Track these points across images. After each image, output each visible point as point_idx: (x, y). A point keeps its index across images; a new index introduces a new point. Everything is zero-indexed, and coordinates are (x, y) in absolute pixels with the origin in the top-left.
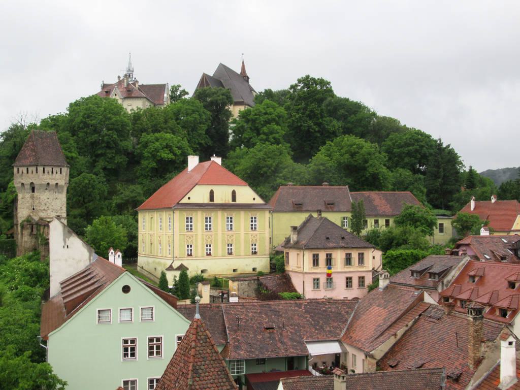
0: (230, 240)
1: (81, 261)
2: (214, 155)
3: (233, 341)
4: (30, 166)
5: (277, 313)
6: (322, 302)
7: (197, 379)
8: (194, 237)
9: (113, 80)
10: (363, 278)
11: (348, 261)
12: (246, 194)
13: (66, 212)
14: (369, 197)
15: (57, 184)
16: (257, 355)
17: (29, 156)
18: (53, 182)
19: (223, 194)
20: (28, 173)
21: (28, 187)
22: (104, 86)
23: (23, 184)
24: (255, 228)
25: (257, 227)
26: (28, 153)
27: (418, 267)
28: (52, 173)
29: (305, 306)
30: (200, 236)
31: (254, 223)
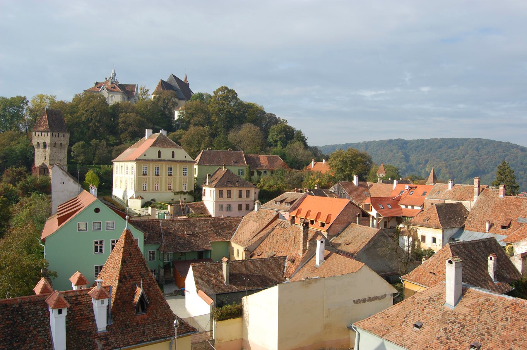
0: (170, 182)
1: (72, 192)
3: (166, 241)
6: (221, 219)
7: (125, 266)
8: (148, 179)
9: (102, 80)
10: (249, 205)
11: (240, 196)
12: (181, 154)
13: (67, 161)
15: (61, 143)
19: (166, 153)
20: (42, 136)
21: (41, 145)
22: (97, 84)
23: (38, 143)
24: (186, 175)
27: (279, 198)
28: (58, 136)
29: (211, 221)
30: (151, 179)
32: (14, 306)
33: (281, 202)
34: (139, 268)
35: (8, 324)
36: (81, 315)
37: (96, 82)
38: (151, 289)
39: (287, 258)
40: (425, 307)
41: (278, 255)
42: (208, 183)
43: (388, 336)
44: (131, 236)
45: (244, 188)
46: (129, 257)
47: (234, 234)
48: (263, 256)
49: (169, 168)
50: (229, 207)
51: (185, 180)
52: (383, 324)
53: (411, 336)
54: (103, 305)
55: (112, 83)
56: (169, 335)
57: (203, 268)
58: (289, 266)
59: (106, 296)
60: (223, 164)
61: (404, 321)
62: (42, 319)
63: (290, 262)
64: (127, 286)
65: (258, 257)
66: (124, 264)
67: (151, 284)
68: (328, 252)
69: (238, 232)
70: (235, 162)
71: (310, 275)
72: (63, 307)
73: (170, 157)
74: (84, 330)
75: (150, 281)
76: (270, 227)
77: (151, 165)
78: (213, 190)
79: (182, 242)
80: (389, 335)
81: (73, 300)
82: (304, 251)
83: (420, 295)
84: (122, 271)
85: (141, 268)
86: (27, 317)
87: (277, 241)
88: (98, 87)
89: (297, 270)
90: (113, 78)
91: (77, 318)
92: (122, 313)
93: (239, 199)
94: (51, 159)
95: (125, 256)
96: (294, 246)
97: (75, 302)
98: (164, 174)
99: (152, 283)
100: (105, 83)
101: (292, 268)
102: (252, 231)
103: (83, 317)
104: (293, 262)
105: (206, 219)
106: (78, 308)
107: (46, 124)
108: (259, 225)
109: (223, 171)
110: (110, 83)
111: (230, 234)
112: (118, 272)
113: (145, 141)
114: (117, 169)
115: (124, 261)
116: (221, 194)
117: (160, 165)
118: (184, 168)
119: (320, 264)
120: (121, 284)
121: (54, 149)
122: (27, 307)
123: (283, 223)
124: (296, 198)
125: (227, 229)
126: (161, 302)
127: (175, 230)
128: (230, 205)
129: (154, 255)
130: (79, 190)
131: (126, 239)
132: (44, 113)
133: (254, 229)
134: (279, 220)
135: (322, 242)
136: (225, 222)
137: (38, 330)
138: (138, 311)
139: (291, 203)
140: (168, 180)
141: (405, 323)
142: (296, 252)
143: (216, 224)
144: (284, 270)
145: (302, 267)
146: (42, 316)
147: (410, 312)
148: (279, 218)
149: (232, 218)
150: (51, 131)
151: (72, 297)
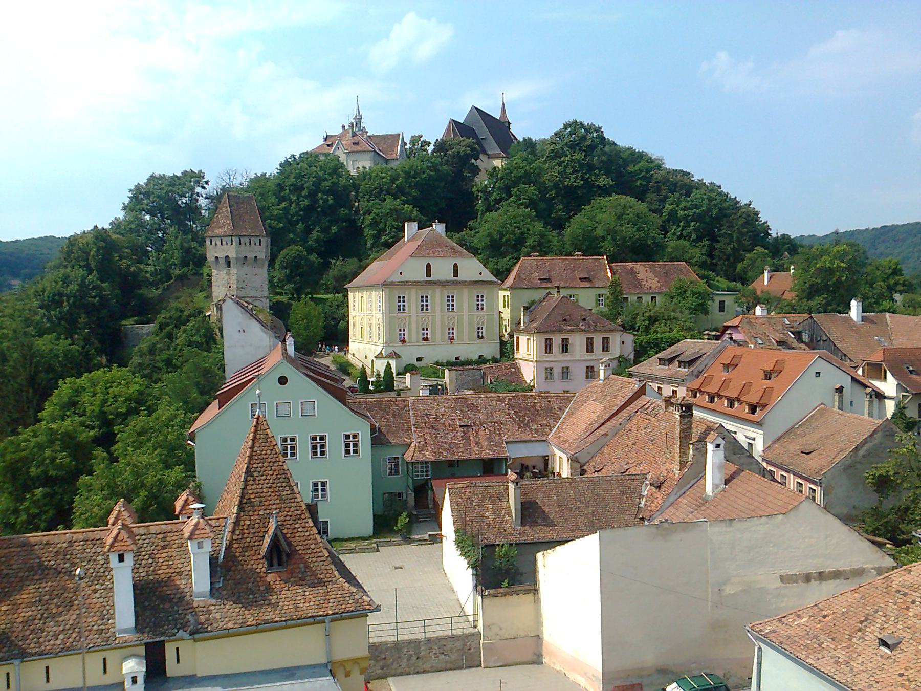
2: (437, 221)
7: (251, 482)
11: (590, 347)
14: (632, 269)
15: (256, 257)
16: (446, 457)
18: (251, 256)
19: (442, 269)
20: (222, 244)
21: (222, 261)
23: (217, 258)
25: (484, 307)
27: (665, 354)
30: (414, 319)
32: (59, 546)
33: (671, 361)
37: (327, 136)
40: (913, 602)
41: (633, 471)
42: (524, 324)
43: (819, 659)
47: (557, 427)
50: (565, 372)
52: (811, 632)
53: (871, 664)
56: (321, 613)
57: (470, 493)
61: (860, 630)
62: (102, 570)
67: (298, 517)
68: (733, 468)
71: (690, 516)
73: (422, 276)
74: (170, 594)
77: (413, 292)
80: (820, 656)
82: (683, 464)
83: (906, 573)
88: (328, 145)
89: (667, 504)
90: (356, 125)
91: (160, 572)
97: (162, 544)
98: (438, 308)
100: (342, 135)
101: (657, 498)
102: (591, 421)
104: (659, 488)
105: (500, 395)
107: (228, 222)
109: (555, 299)
113: (405, 244)
114: (354, 302)
119: (713, 492)
121: (246, 269)
123: (651, 404)
124: (704, 351)
133: (594, 416)
134: (644, 399)
135: (718, 446)
136: (538, 403)
137: (93, 588)
139: (691, 363)
141: (859, 634)
144: (640, 503)
147: (877, 611)
148: (645, 394)
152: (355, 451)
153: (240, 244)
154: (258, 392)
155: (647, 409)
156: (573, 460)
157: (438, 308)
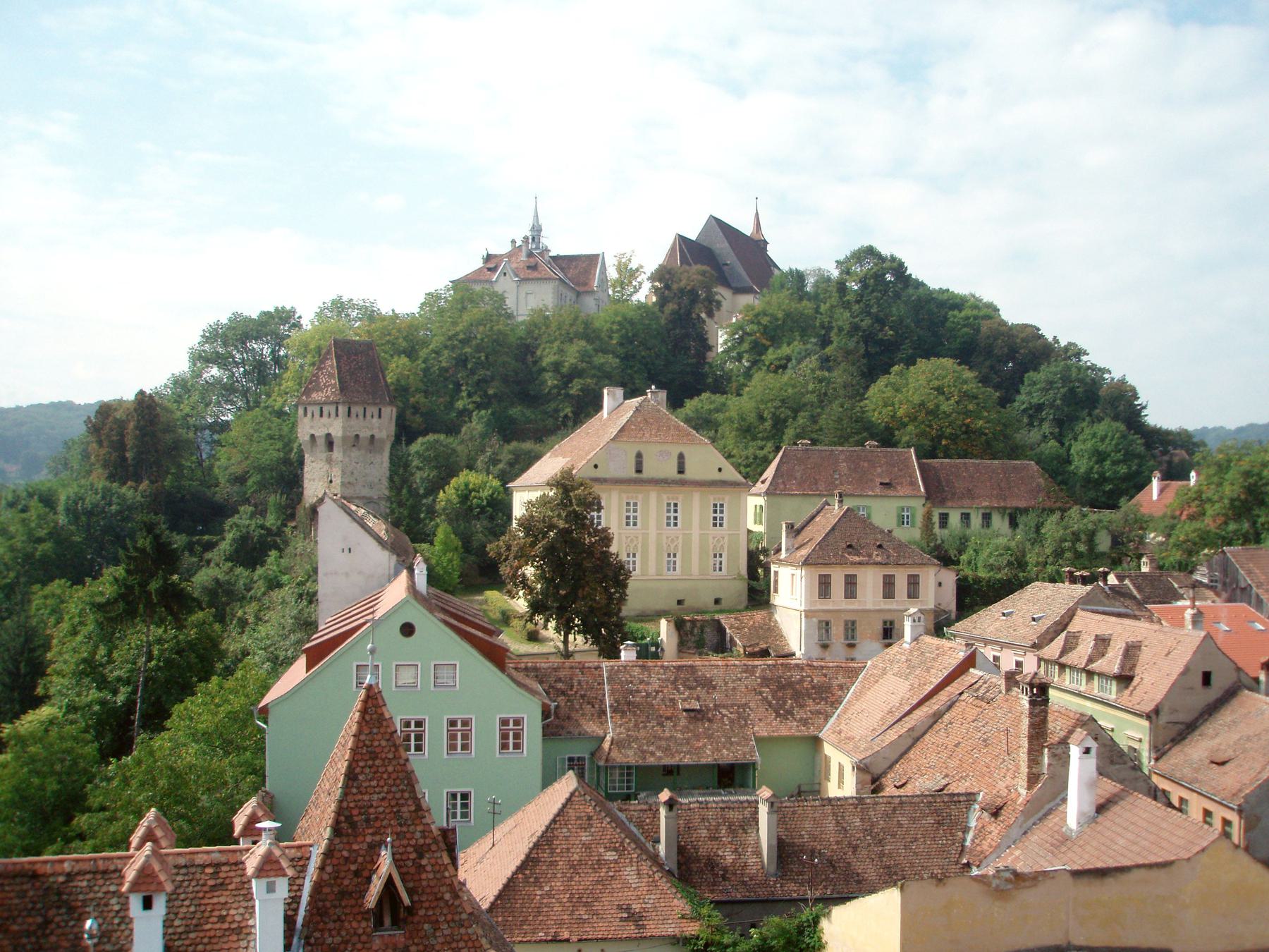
0: (672, 546)
4: (325, 403)
5: (708, 684)
7: (354, 791)
9: (502, 248)
15: (373, 436)
16: (660, 758)
17: (326, 386)
20: (321, 416)
21: (321, 442)
22: (489, 258)
23: (313, 436)
25: (725, 521)
26: (323, 380)
29: (763, 670)
31: (718, 515)
34: (394, 798)
35: (30, 924)
36: (222, 919)
38: (424, 862)
39: (980, 798)
41: (954, 788)
42: (787, 550)
44: (381, 703)
45: (901, 570)
46: (370, 763)
48: (908, 790)
49: (669, 505)
51: (632, 541)
54: (272, 896)
55: (530, 255)
58: (983, 827)
59: (282, 869)
60: (836, 492)
62: (117, 921)
63: (986, 814)
64: (355, 847)
65: (897, 792)
66: (350, 783)
69: (844, 712)
70: (887, 484)
72: (154, 891)
75: (425, 837)
76: (943, 697)
78: (799, 573)
79: (667, 734)
81: (207, 874)
82: (1033, 779)
84: (345, 805)
85: (402, 797)
86: (80, 910)
87: (959, 743)
88: (489, 269)
90: (533, 239)
92: (331, 925)
93: (885, 603)
94: (347, 481)
95: (357, 761)
96: (1004, 761)
97: (211, 882)
98: (652, 523)
99: (429, 845)
100: (510, 255)
101: (990, 833)
103: (226, 926)
104: (996, 814)
106: (215, 900)
108: (912, 688)
110: (523, 257)
111: (821, 713)
112: (333, 806)
115: (351, 776)
116: (824, 587)
117: (640, 496)
118: (715, 505)
120: (337, 841)
121: (355, 453)
122: (85, 883)
123: (985, 683)
125: (814, 700)
126: (450, 903)
127: (648, 695)
128: (853, 623)
129: (583, 769)
130: (392, 571)
131: (364, 711)
132: (328, 352)
133: (894, 701)
138: (379, 924)
140: (665, 540)
142: (1008, 781)
143: (779, 682)
144: (964, 840)
145: (1025, 833)
146: (118, 912)
148: (974, 667)
149: (831, 664)
150: (344, 403)
151: (204, 866)
152: (517, 746)
153: (349, 415)
154: (370, 646)
155: (978, 689)
156: (861, 768)
157: (652, 523)
